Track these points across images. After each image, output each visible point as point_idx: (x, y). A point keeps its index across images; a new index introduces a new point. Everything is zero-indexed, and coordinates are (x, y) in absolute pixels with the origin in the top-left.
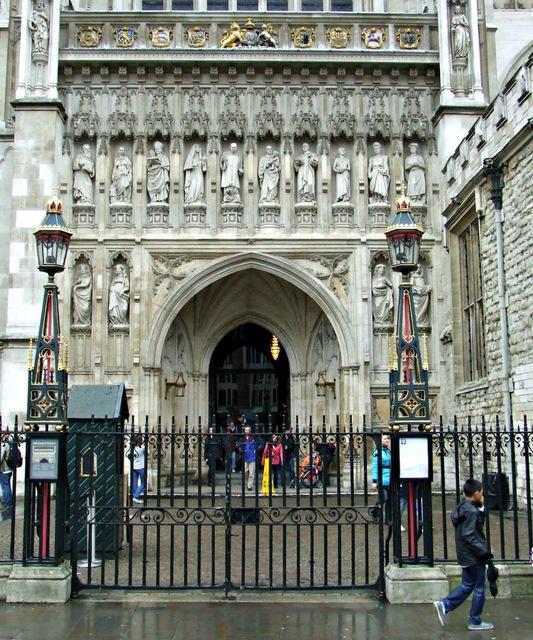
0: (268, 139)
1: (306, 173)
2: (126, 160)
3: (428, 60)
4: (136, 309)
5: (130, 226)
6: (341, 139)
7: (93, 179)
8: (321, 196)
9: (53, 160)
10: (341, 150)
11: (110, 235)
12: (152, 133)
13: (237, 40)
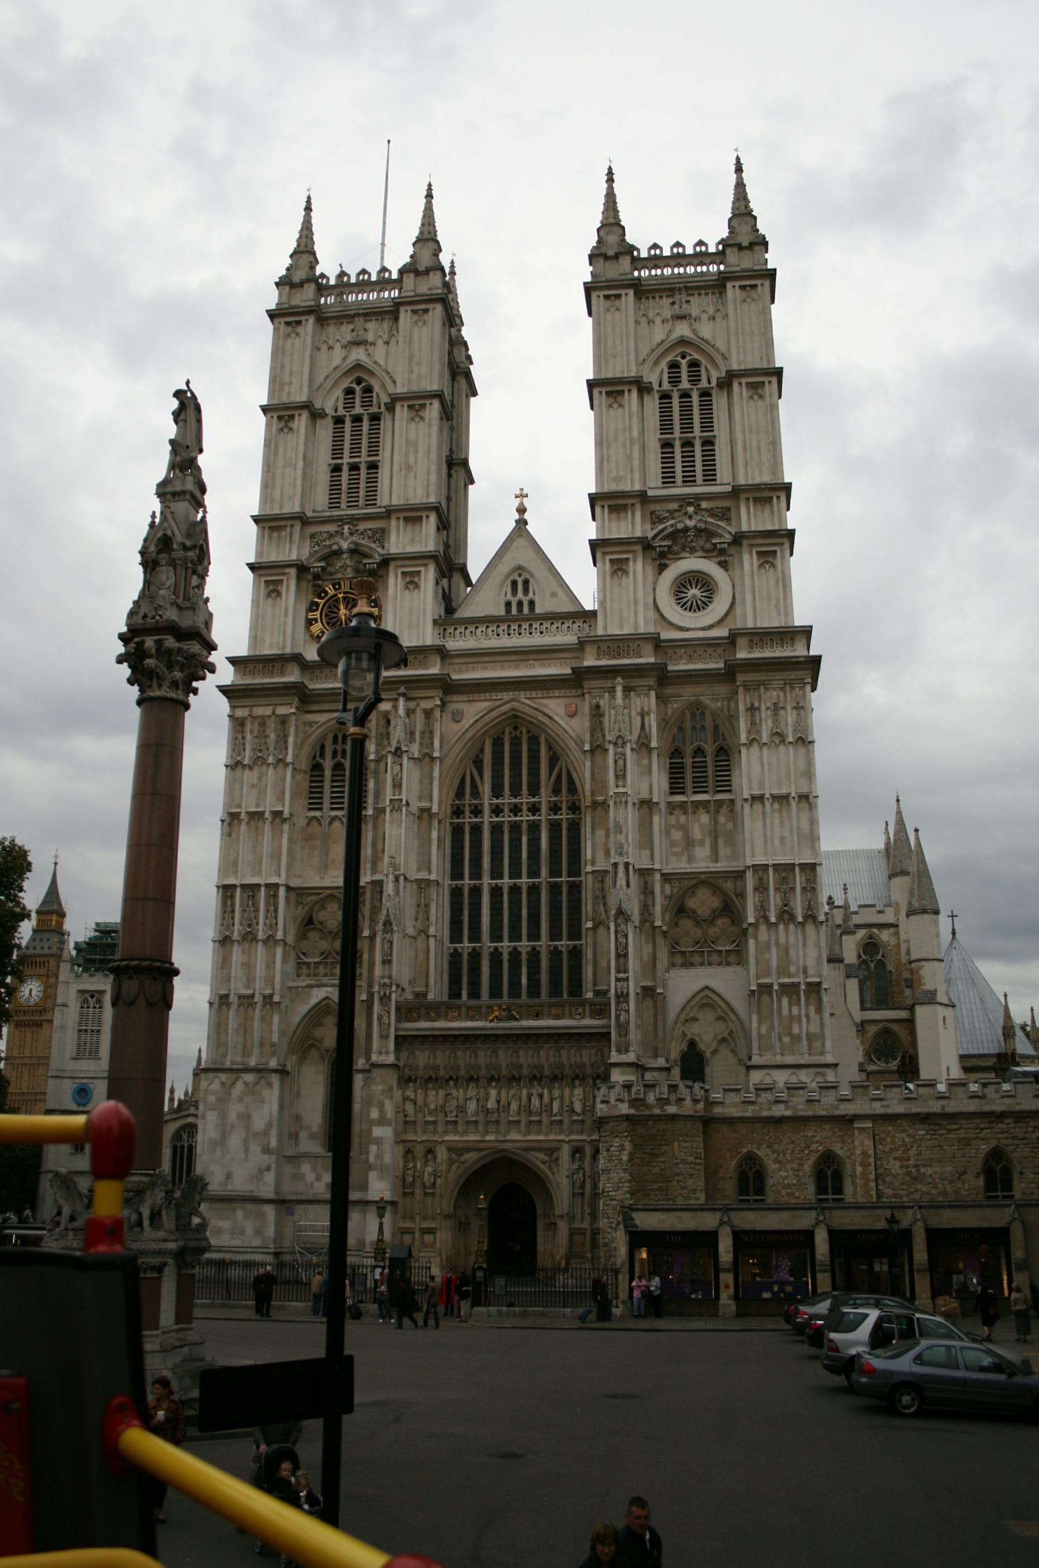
0: (512, 1079)
1: (536, 1102)
2: (434, 1092)
3: (605, 1030)
4: (439, 1181)
5: (435, 1132)
6: (555, 1078)
7: (415, 1104)
8: (544, 1114)
9: (392, 1097)
10: (556, 1085)
11: (425, 1138)
12: (447, 1077)
13: (496, 1017)
